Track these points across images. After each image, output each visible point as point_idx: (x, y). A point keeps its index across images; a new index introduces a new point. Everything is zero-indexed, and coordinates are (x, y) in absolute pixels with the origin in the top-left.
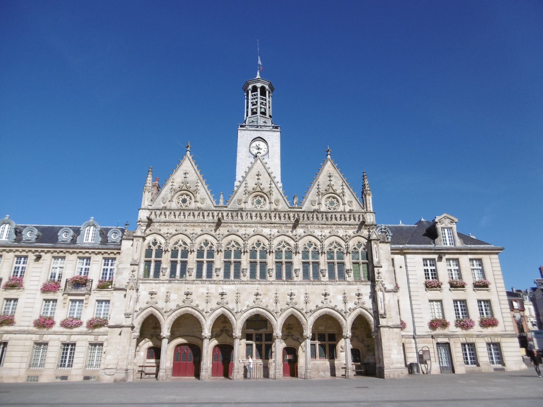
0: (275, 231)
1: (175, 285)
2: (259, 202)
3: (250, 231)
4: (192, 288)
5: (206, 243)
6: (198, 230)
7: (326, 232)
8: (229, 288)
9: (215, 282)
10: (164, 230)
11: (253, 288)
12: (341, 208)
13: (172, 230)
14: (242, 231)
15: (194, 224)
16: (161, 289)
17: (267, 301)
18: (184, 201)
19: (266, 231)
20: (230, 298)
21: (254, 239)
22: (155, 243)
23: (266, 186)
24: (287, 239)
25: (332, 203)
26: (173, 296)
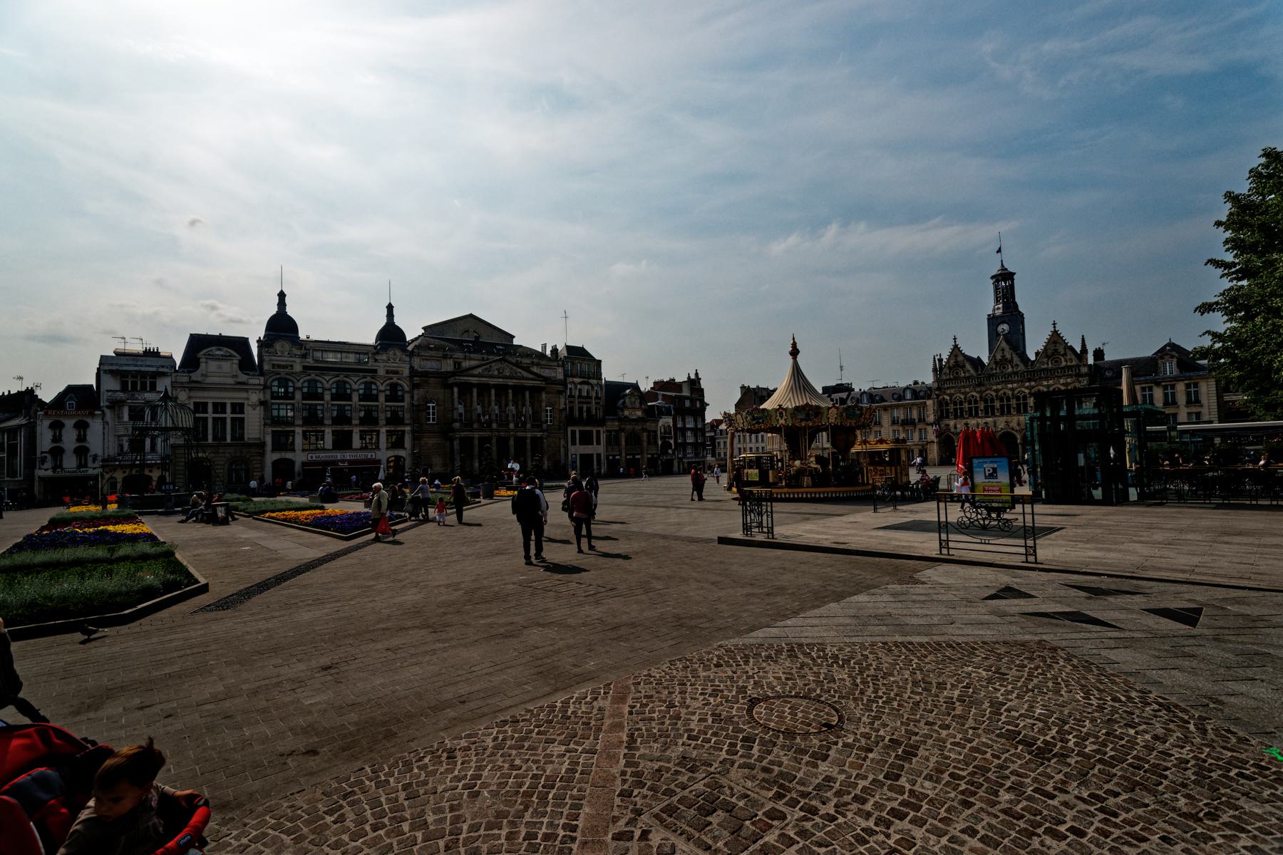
0: (1015, 385)
1: (958, 420)
2: (1004, 368)
3: (999, 387)
4: (969, 421)
5: (973, 396)
6: (967, 390)
7: (1051, 382)
8: (990, 420)
9: (980, 417)
10: (948, 392)
11: (1003, 419)
12: (1064, 364)
13: (953, 391)
14: (995, 387)
15: (964, 387)
16: (952, 423)
17: (1014, 424)
18: (957, 373)
19: (1010, 386)
20: (991, 425)
21: (1002, 392)
22: (944, 399)
23: (1008, 356)
24: (1023, 389)
25: (1056, 362)
26: (958, 426)
